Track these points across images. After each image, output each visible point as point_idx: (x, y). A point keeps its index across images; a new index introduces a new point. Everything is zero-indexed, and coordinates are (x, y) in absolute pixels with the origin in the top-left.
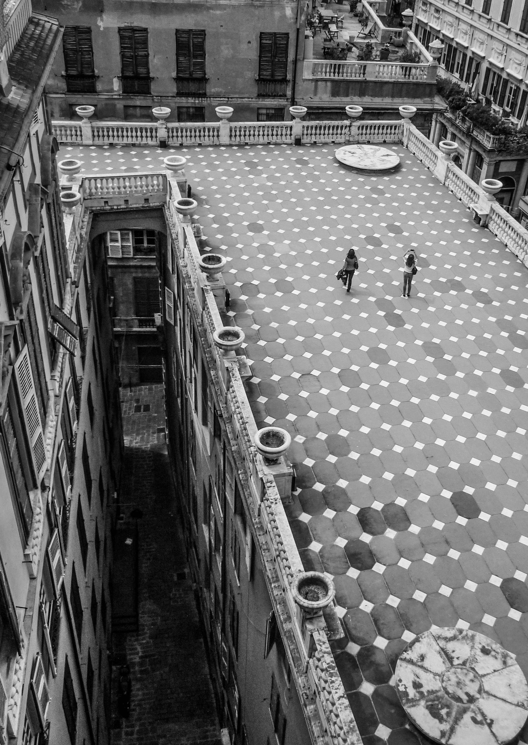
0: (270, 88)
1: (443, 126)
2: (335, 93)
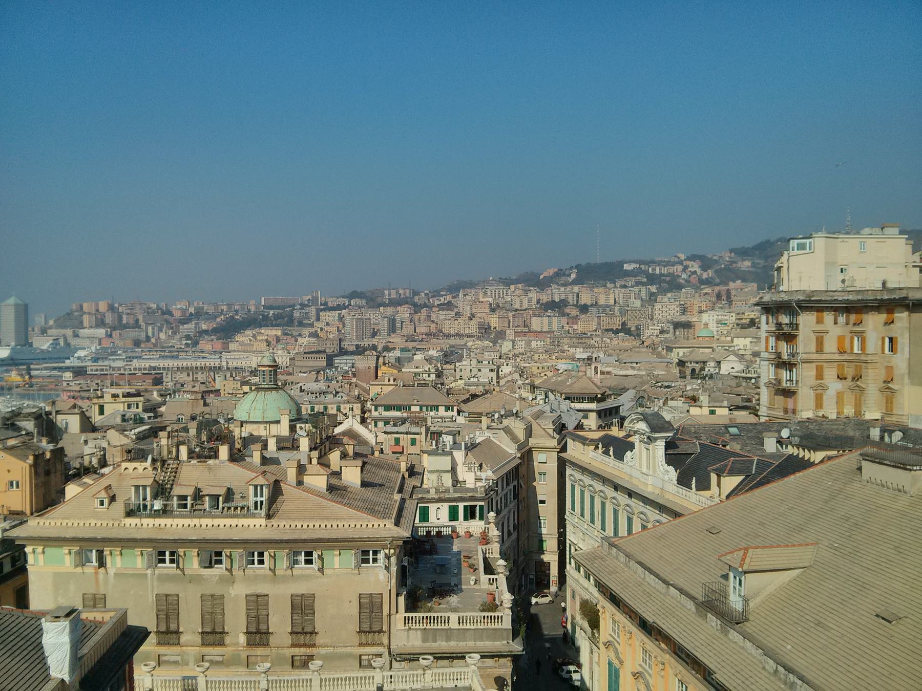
0: (369, 638)
2: (425, 640)
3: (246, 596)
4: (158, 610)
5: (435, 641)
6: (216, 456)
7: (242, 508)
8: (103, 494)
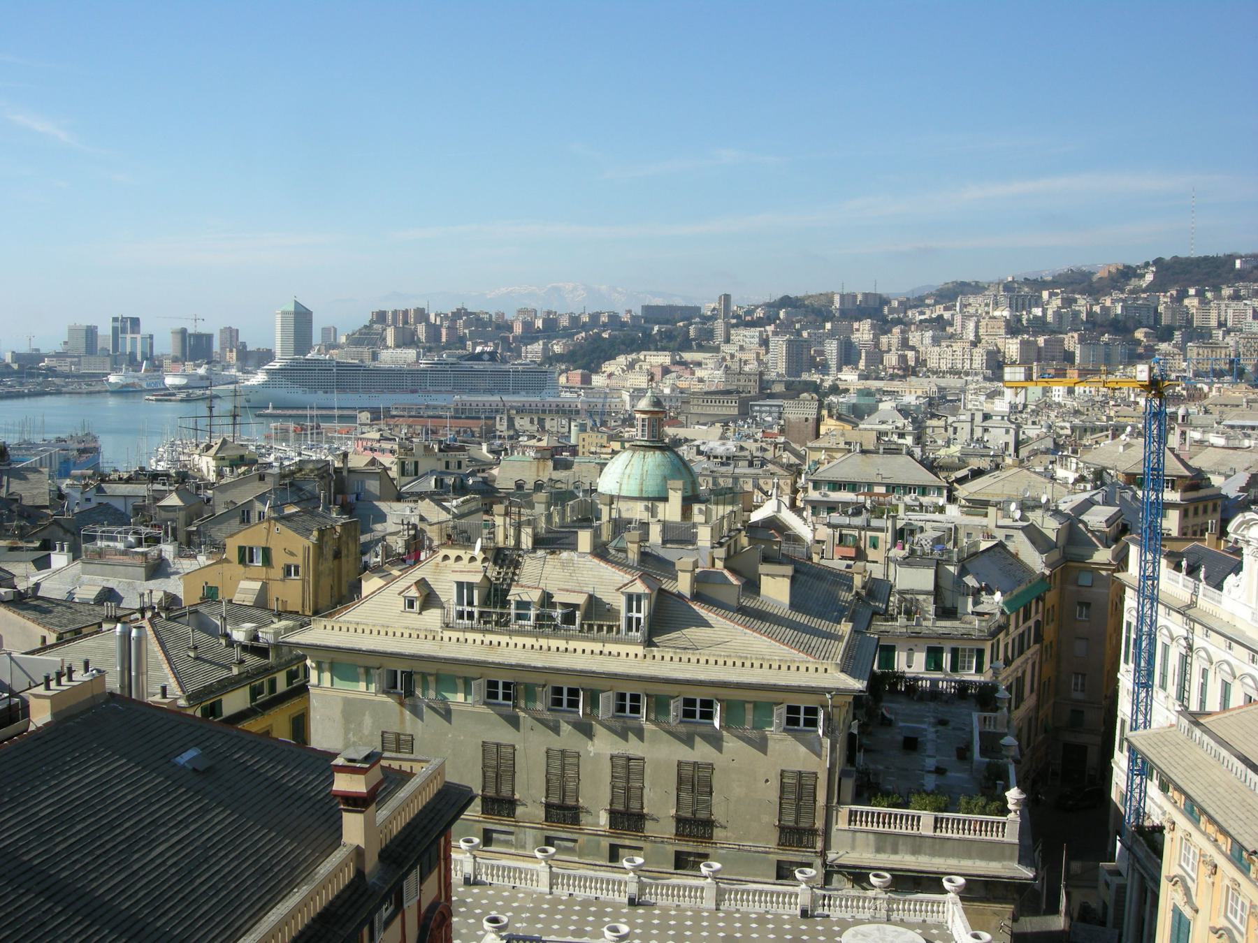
1: (1142, 878)
3: (612, 757)
4: (484, 766)
5: (895, 852)
6: (573, 547)
7: (610, 628)
8: (414, 592)
